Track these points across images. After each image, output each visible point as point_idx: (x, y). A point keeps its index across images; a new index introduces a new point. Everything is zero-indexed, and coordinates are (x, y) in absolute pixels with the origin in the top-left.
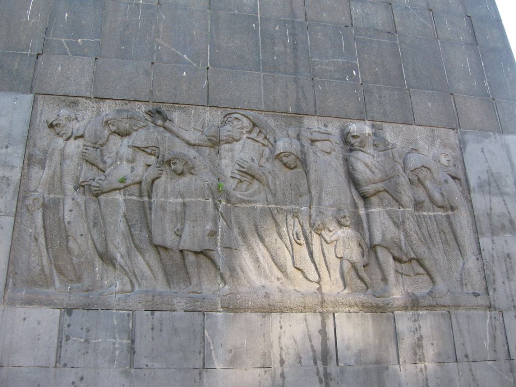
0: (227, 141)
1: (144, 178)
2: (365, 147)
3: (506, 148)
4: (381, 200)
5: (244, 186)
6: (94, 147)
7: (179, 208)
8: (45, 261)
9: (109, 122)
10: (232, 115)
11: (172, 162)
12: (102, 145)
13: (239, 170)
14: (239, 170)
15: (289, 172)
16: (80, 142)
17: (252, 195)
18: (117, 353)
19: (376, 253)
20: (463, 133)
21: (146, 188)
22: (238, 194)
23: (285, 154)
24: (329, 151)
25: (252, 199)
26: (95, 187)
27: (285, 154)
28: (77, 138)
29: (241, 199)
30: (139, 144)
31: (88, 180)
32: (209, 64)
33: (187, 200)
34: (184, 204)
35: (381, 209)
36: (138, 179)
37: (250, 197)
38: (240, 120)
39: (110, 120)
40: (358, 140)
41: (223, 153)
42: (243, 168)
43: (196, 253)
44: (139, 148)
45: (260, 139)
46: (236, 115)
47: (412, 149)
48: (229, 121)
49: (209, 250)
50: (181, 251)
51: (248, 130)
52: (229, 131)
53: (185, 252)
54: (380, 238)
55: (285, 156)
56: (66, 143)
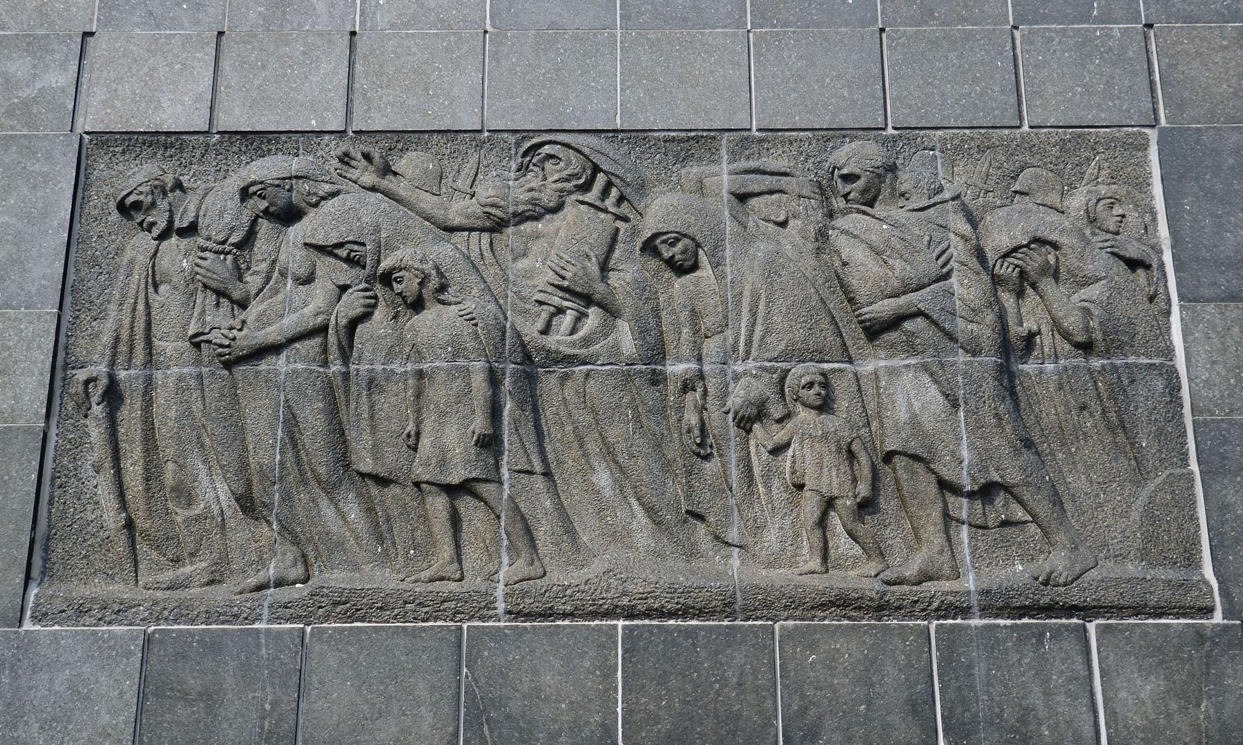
0: (527, 214)
1: (333, 319)
2: (877, 204)
5: (568, 319)
11: (394, 276)
13: (553, 285)
14: (553, 285)
17: (587, 342)
23: (665, 237)
24: (782, 218)
26: (221, 346)
27: (665, 237)
30: (320, 240)
31: (206, 331)
32: (488, 21)
34: (420, 375)
36: (320, 319)
37: (581, 347)
38: (560, 159)
39: (253, 183)
40: (860, 183)
42: (563, 278)
44: (321, 249)
46: (547, 149)
47: (1016, 192)
48: (534, 165)
49: (477, 480)
50: (417, 484)
51: (582, 181)
52: (531, 190)
53: (424, 486)
55: (665, 242)
56: (160, 244)
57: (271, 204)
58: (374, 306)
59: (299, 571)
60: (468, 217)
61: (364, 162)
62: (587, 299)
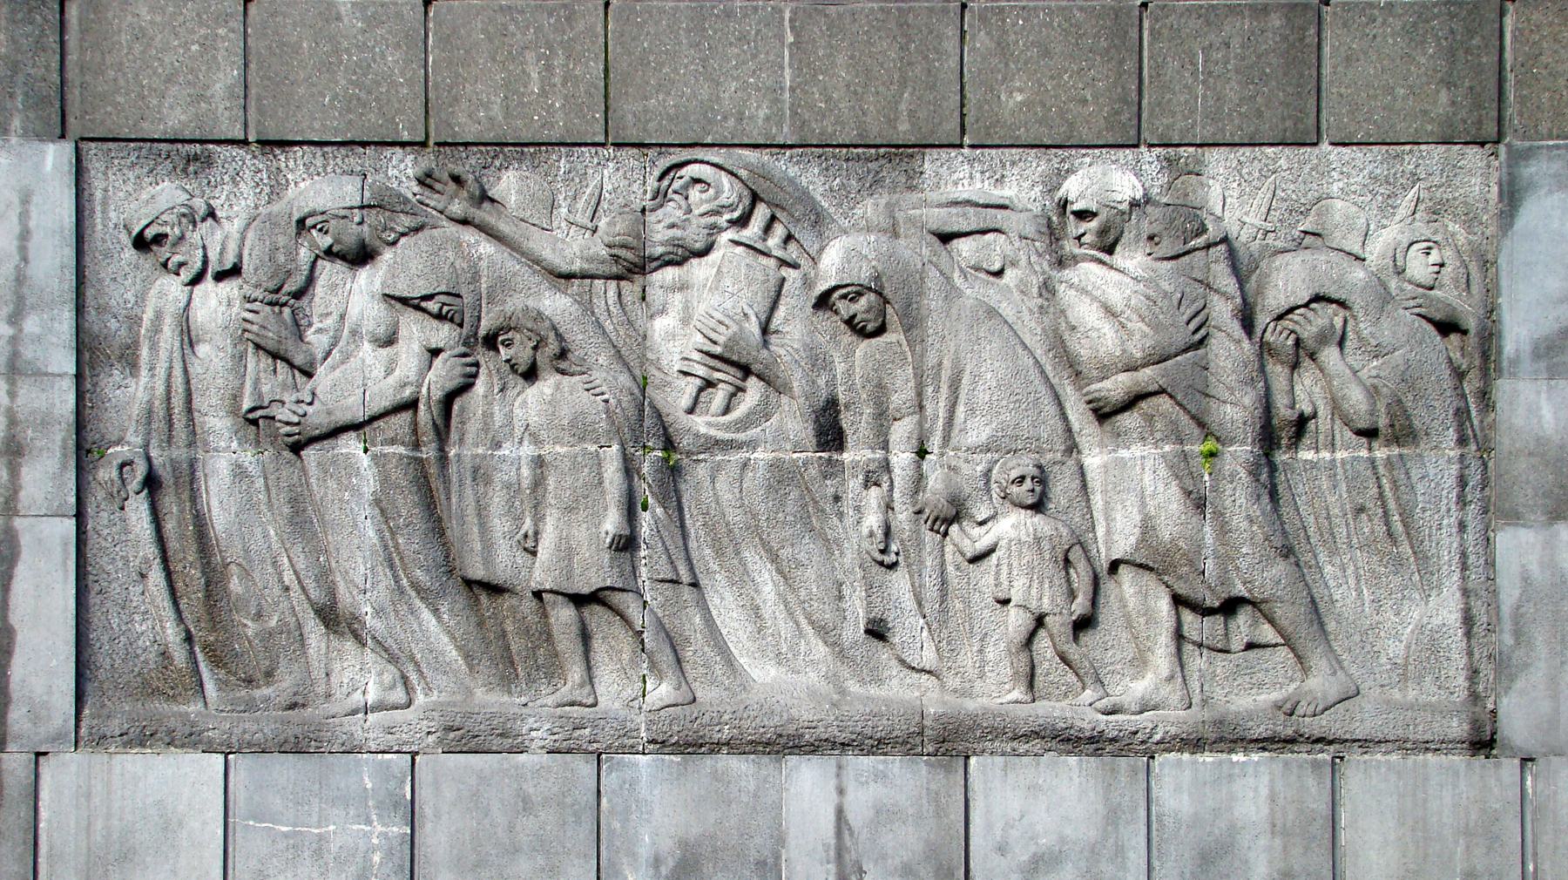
5: (719, 396)
6: (270, 304)
9: (309, 222)
10: (684, 171)
12: (298, 295)
15: (864, 346)
16: (230, 288)
17: (744, 424)
18: (377, 858)
22: (700, 424)
24: (996, 267)
25: (741, 436)
28: (220, 276)
29: (707, 438)
30: (402, 289)
36: (407, 393)
40: (1094, 224)
41: (654, 294)
50: (538, 595)
54: (1133, 540)
57: (337, 241)
58: (475, 376)
59: (399, 695)
60: (590, 260)
61: (452, 186)
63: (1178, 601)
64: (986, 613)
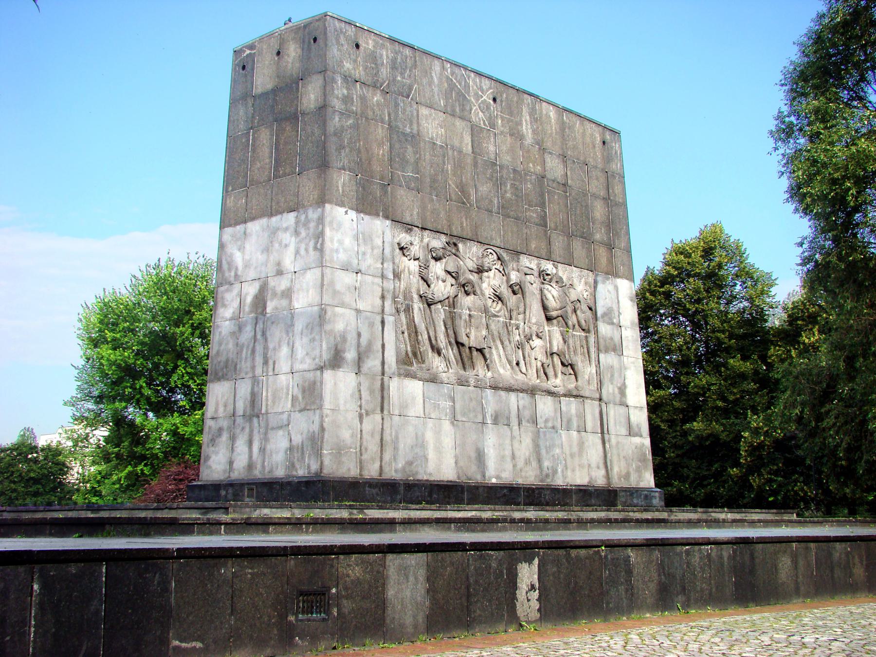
3: (616, 288)
4: (558, 322)
7: (467, 317)
8: (409, 349)
16: (417, 262)
17: (498, 312)
19: (552, 358)
20: (597, 275)
21: (452, 303)
30: (449, 269)
33: (472, 313)
35: (557, 328)
40: (549, 277)
41: (484, 278)
43: (477, 350)
45: (501, 270)
50: (470, 348)
59: (446, 370)
61: (453, 246)
62: (500, 299)
63: (563, 364)
64: (533, 361)
